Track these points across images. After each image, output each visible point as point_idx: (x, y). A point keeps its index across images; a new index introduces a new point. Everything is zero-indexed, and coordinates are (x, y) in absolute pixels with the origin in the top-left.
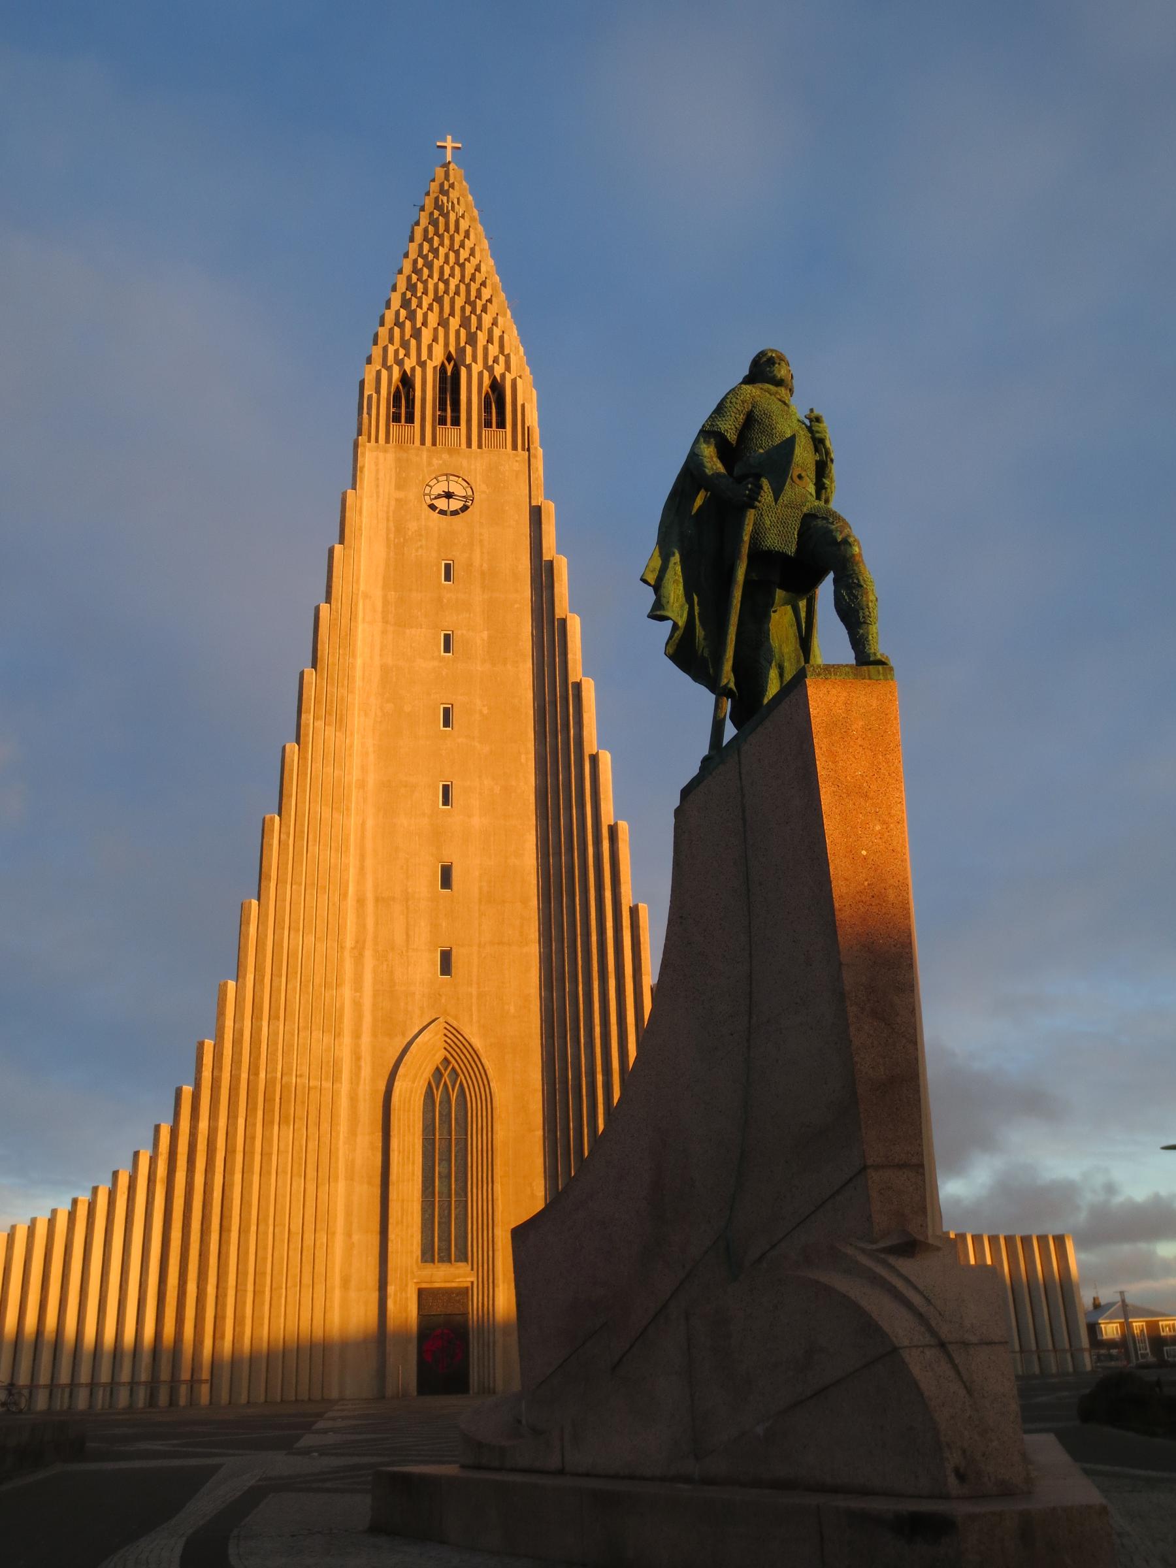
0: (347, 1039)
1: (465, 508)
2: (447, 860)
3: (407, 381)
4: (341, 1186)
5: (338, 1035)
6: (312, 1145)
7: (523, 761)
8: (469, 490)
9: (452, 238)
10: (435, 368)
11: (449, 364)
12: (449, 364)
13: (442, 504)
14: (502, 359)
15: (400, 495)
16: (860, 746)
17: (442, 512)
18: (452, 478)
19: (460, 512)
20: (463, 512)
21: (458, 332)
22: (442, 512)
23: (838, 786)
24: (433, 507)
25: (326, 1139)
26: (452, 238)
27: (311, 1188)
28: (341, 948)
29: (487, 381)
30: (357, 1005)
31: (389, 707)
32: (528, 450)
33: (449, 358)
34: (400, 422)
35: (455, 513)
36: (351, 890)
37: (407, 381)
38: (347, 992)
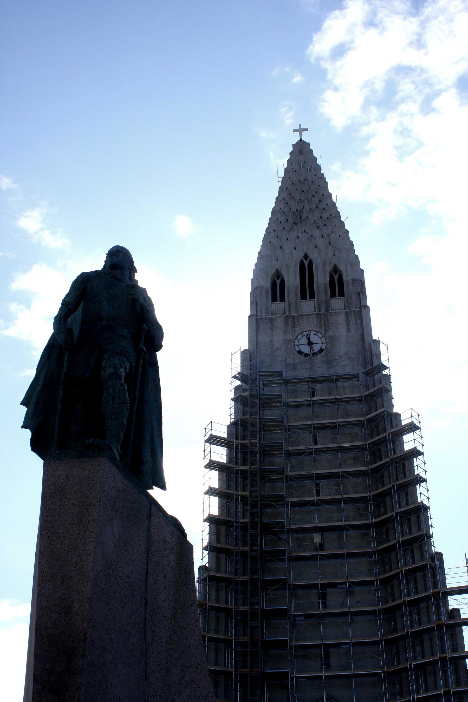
1: (321, 351)
3: (278, 275)
8: (324, 340)
11: (306, 261)
12: (306, 261)
14: (337, 253)
16: (72, 504)
18: (312, 332)
19: (318, 353)
20: (320, 353)
22: (306, 355)
23: (52, 532)
29: (329, 268)
33: (306, 257)
35: (315, 354)
37: (278, 275)
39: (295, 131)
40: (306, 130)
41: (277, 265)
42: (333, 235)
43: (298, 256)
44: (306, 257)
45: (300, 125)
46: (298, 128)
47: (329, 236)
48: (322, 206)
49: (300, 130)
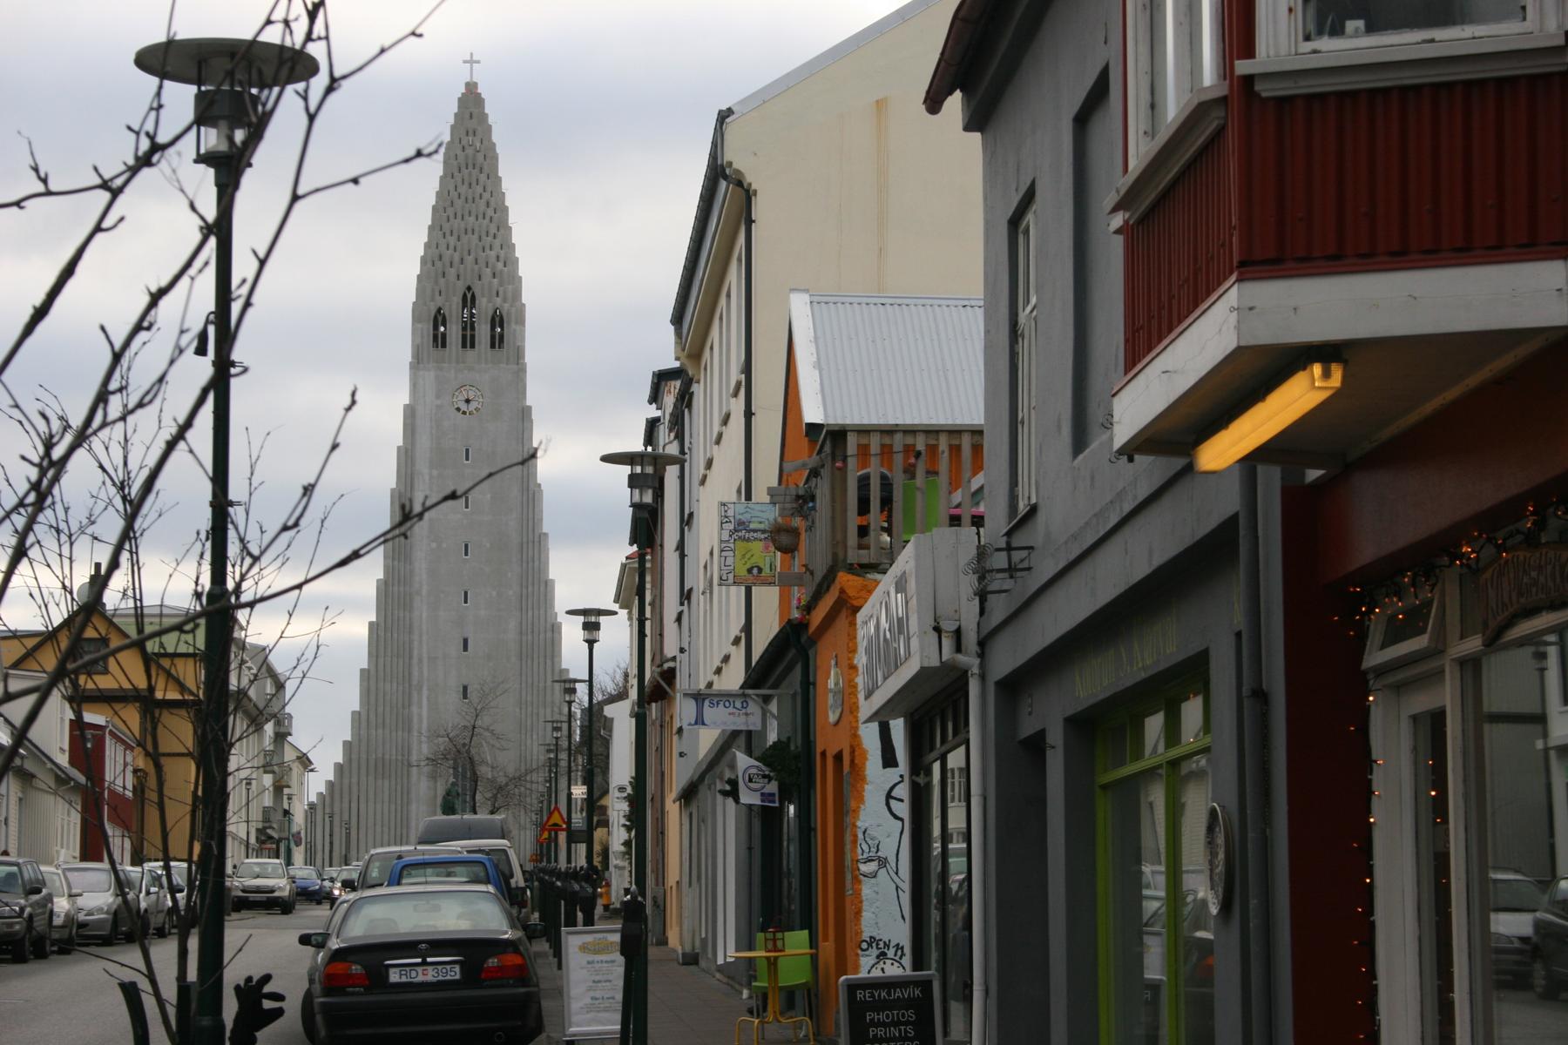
0: (415, 734)
1: (477, 409)
2: (466, 636)
4: (413, 807)
5: (409, 732)
6: (399, 788)
7: (509, 574)
9: (470, 174)
10: (458, 303)
13: (464, 407)
14: (501, 293)
15: (439, 402)
17: (464, 413)
21: (473, 270)
22: (464, 413)
24: (458, 409)
25: (405, 785)
26: (470, 174)
27: (399, 808)
28: (410, 686)
29: (490, 313)
30: (420, 716)
31: (434, 545)
32: (518, 364)
33: (469, 288)
34: (437, 347)
36: (415, 653)
38: (415, 709)
39: (465, 62)
40: (478, 62)
41: (439, 301)
42: (499, 263)
43: (460, 287)
44: (469, 288)
45: (472, 54)
46: (469, 59)
47: (494, 267)
48: (490, 212)
49: (471, 62)
